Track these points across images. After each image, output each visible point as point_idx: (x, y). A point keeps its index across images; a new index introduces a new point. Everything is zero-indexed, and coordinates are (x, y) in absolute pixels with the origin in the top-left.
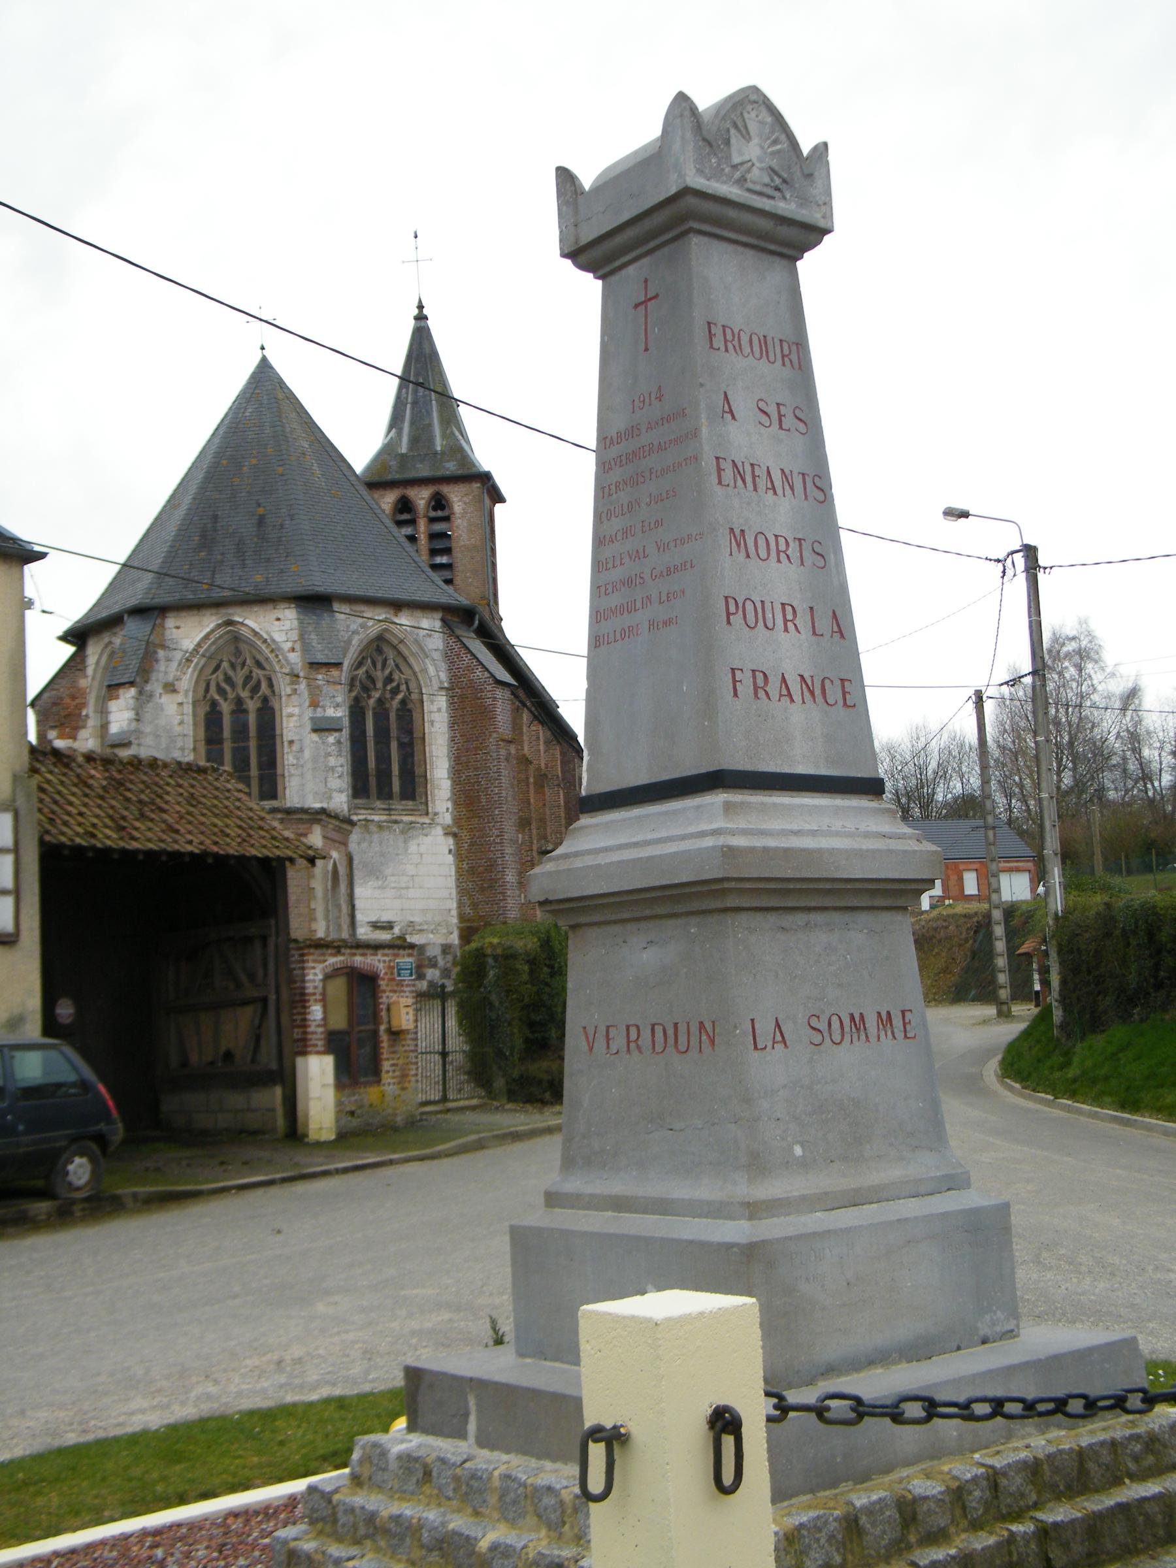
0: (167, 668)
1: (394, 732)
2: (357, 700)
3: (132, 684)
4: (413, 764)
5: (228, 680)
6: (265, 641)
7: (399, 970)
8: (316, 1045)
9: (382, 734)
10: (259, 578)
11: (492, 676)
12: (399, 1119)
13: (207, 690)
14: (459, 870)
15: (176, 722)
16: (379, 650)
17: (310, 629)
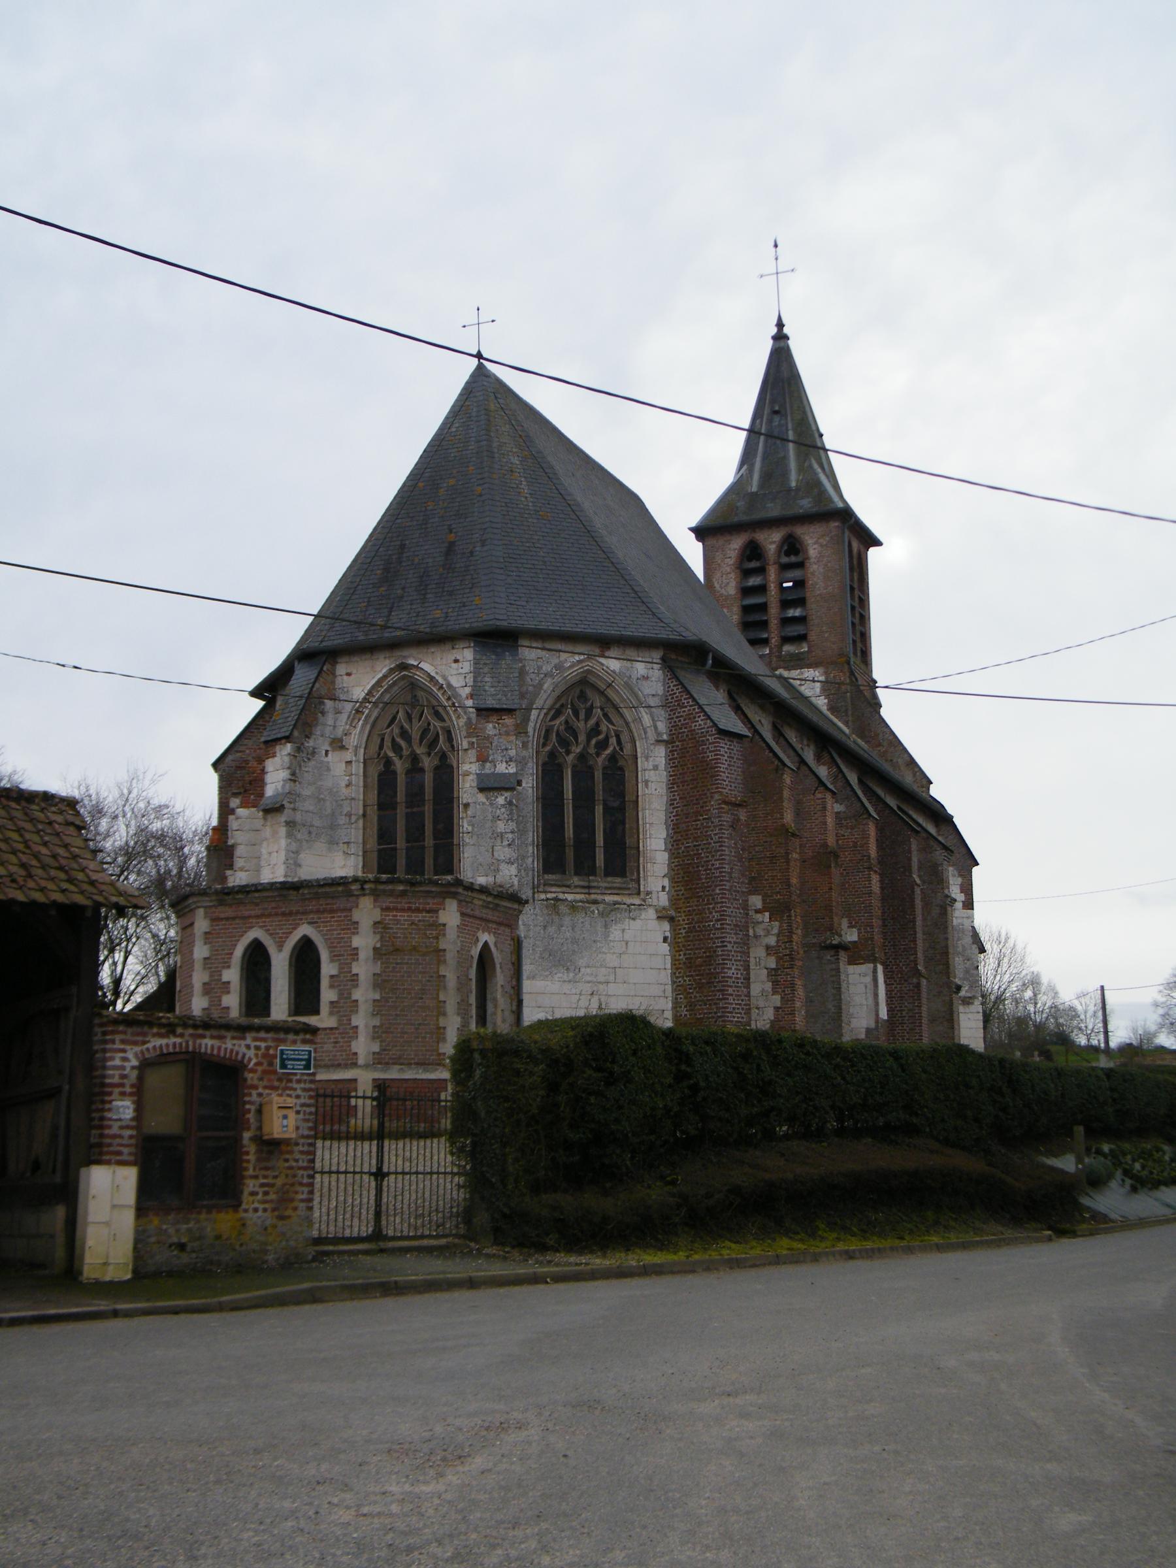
0: (336, 720)
1: (599, 794)
2: (552, 755)
3: (288, 738)
4: (624, 830)
5: (404, 734)
6: (441, 687)
7: (283, 1061)
8: (119, 1153)
9: (584, 798)
10: (438, 614)
11: (715, 725)
12: (270, 1257)
13: (381, 747)
14: (675, 962)
15: (343, 784)
16: (582, 696)
17: (486, 670)
